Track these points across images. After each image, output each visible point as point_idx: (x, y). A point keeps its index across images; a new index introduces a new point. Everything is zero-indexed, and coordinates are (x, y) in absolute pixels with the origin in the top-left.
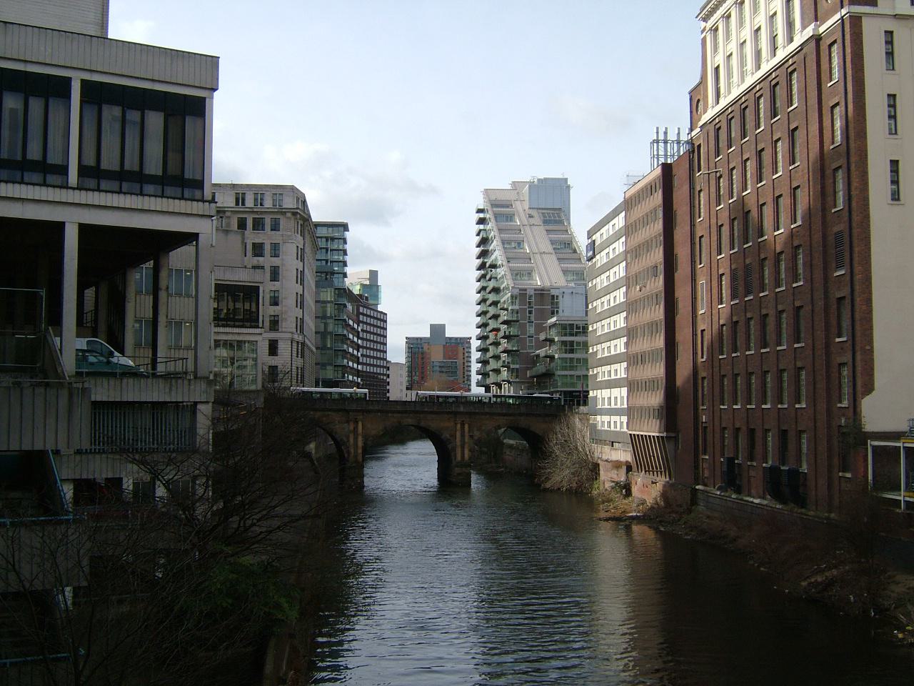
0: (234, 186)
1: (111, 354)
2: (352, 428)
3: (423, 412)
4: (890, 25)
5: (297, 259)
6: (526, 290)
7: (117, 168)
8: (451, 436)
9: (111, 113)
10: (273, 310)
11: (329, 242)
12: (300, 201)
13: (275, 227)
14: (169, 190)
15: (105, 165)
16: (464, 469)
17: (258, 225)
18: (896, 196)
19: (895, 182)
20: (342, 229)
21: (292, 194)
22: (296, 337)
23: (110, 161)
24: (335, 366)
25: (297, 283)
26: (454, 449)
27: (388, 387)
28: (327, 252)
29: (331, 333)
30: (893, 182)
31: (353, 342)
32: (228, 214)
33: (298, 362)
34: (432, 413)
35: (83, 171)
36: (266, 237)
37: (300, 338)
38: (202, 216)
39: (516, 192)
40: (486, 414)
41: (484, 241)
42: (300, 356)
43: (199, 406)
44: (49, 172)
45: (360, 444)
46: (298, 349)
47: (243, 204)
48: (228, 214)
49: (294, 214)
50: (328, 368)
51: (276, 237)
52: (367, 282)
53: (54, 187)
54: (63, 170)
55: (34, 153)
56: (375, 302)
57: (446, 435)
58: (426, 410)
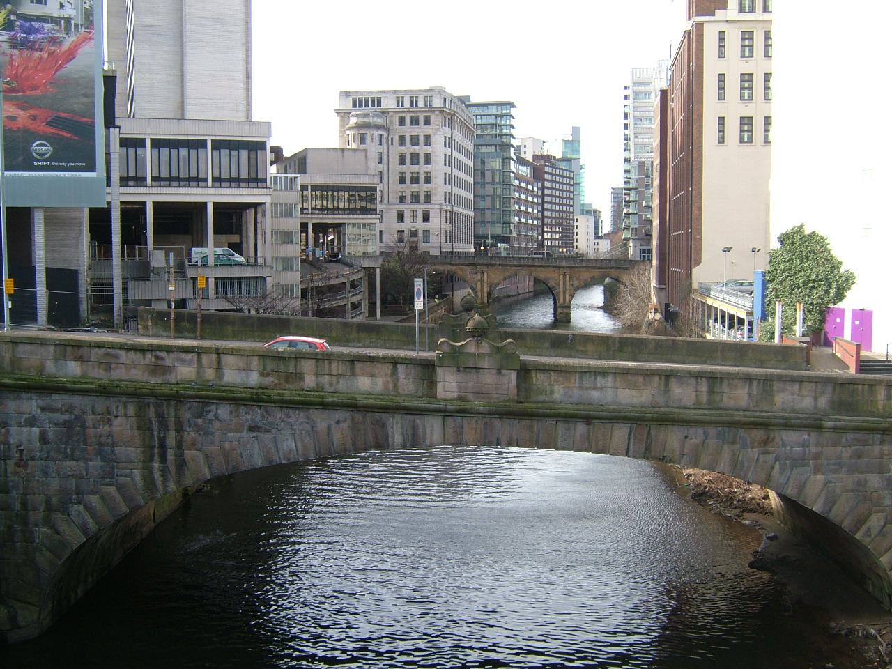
0: (395, 92)
1: (233, 255)
2: (479, 277)
3: (534, 266)
4: (723, 27)
5: (445, 146)
6: (644, 162)
7: (229, 177)
8: (556, 284)
9: (225, 152)
10: (426, 187)
11: (498, 119)
12: (447, 100)
13: (427, 122)
14: (251, 184)
15: (223, 176)
16: (565, 310)
17: (415, 121)
18: (721, 140)
19: (721, 131)
20: (508, 107)
21: (439, 96)
22: (444, 207)
23: (225, 175)
24: (504, 224)
25: (445, 165)
26: (558, 293)
27: (575, 237)
28: (496, 128)
29: (499, 196)
30: (719, 131)
31: (527, 201)
32: (391, 114)
33: (448, 226)
34: (540, 266)
35: (214, 179)
36: (421, 130)
37: (449, 208)
38: (267, 195)
39: (659, 70)
40: (583, 267)
41: (626, 116)
42: (448, 222)
43: (267, 278)
44: (198, 180)
45: (486, 289)
46: (446, 217)
47: (402, 105)
48: (391, 114)
49: (441, 112)
50: (498, 225)
51: (428, 130)
52: (570, 138)
53: (202, 187)
54: (205, 180)
55: (193, 174)
56: (577, 157)
57: (551, 284)
58: (536, 264)
